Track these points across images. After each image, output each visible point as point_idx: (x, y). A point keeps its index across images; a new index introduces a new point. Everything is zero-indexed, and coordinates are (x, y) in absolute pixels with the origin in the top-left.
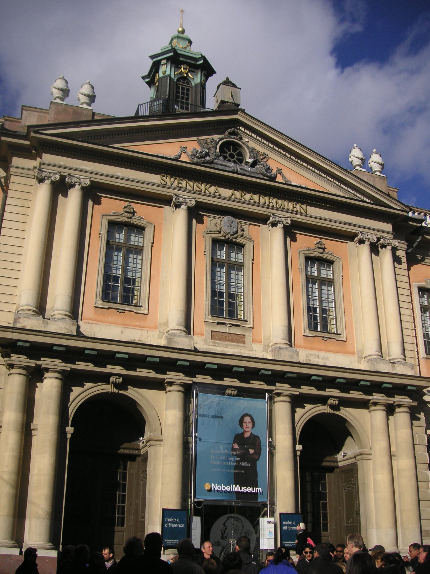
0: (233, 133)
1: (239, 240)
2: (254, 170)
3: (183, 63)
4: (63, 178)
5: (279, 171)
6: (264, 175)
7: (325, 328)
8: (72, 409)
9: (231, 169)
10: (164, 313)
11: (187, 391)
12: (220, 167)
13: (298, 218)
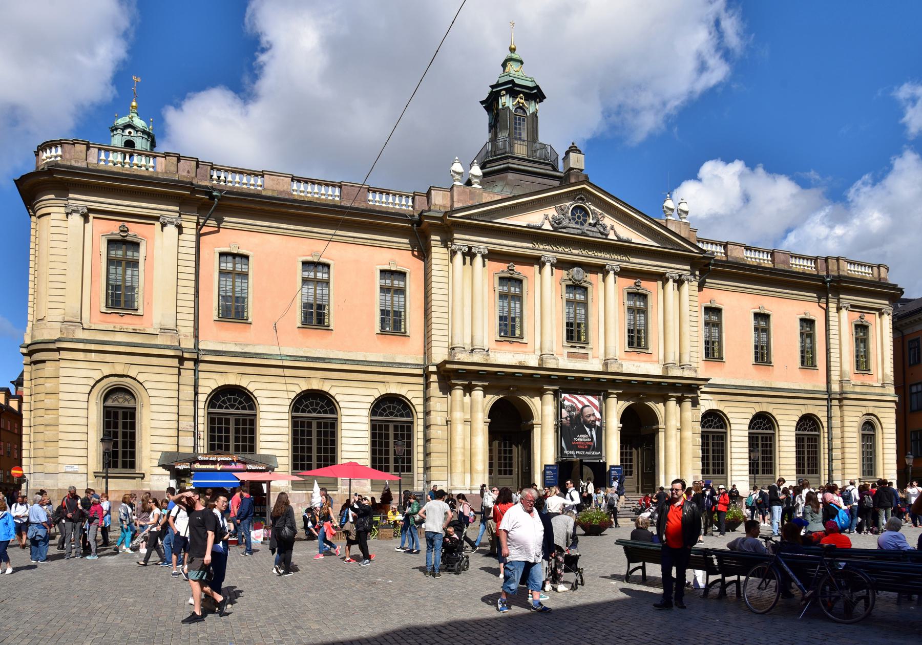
1: (584, 284)
2: (595, 229)
4: (470, 248)
6: (602, 233)
7: (639, 344)
9: (579, 231)
10: (542, 343)
12: (572, 231)
13: (625, 265)
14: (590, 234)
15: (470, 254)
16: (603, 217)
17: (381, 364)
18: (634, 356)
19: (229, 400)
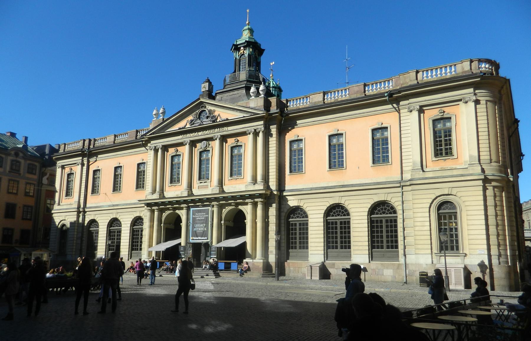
0: (202, 107)
1: (208, 149)
2: (207, 120)
3: (240, 48)
5: (219, 115)
11: (188, 208)
14: (204, 123)
15: (156, 151)
16: (214, 111)
17: (135, 204)
18: (233, 182)
19: (382, 209)
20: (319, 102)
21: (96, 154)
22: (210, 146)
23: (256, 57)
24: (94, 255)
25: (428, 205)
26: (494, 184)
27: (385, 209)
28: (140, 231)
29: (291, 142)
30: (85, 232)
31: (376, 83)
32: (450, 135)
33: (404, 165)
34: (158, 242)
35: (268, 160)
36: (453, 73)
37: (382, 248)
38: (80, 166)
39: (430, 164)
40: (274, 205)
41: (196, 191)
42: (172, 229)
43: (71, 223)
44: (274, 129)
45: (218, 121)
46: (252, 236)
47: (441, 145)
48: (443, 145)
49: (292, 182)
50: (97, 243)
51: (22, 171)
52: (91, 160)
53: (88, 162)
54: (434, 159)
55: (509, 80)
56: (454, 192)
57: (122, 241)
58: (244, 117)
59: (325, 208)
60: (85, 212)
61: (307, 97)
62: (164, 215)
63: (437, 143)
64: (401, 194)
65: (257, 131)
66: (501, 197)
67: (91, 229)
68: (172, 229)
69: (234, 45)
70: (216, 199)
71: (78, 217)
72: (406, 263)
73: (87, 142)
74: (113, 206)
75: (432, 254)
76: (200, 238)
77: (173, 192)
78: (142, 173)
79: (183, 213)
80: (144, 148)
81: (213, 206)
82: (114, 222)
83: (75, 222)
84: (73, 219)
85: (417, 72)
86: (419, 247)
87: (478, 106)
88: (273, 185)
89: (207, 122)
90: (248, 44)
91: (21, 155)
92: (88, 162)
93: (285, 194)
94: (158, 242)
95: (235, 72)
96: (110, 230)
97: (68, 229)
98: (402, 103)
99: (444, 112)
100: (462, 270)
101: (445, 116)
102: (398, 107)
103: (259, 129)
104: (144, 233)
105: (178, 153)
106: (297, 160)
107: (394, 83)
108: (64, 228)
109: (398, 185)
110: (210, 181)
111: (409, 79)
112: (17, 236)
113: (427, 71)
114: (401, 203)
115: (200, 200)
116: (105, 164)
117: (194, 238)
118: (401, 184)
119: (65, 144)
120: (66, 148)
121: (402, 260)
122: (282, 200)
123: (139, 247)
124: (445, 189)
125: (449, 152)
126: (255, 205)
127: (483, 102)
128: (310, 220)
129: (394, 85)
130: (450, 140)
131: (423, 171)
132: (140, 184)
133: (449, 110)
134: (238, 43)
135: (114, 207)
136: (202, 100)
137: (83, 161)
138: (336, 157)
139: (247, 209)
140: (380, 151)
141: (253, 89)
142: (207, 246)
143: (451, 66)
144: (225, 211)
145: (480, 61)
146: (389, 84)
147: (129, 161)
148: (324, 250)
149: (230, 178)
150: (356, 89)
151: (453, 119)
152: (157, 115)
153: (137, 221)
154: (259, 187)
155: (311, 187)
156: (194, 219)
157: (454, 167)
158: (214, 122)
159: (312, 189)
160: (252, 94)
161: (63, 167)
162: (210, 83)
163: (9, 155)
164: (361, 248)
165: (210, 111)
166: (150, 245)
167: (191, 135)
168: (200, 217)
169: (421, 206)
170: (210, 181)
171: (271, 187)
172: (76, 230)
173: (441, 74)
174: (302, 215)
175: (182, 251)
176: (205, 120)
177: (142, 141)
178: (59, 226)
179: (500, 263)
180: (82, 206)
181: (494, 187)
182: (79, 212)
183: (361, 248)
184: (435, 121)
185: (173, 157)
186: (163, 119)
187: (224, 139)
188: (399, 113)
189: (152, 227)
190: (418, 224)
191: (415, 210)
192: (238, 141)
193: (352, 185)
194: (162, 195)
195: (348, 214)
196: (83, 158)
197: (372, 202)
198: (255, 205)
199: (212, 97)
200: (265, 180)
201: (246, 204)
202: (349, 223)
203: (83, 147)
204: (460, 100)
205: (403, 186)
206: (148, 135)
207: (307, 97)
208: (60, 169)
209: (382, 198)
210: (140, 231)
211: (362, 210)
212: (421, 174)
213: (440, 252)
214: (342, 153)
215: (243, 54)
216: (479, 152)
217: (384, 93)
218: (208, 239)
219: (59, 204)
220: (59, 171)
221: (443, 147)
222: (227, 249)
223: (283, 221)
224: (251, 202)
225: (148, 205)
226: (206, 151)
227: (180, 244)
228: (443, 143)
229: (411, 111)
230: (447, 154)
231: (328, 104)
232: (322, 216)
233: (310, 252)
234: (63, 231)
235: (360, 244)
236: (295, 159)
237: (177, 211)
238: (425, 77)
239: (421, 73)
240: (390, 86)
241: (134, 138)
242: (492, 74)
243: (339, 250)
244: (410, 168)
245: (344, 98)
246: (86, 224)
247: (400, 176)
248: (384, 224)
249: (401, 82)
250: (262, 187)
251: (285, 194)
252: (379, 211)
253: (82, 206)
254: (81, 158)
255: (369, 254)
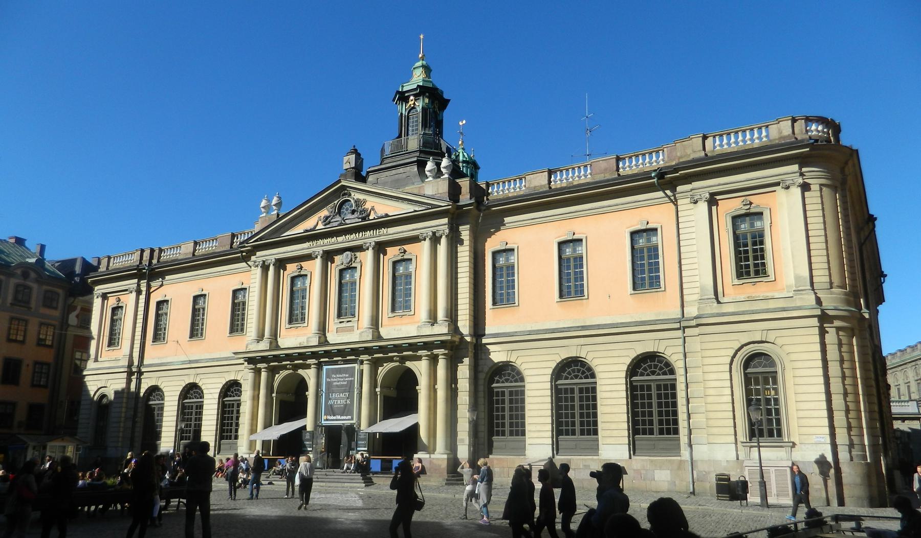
2: (353, 216)
3: (409, 97)
4: (264, 262)
5: (373, 209)
8: (276, 385)
11: (319, 366)
14: (347, 221)
15: (265, 268)
16: (365, 201)
18: (397, 320)
19: (650, 367)
20: (541, 186)
21: (162, 275)
22: (358, 260)
23: (435, 112)
24: (155, 447)
25: (728, 360)
26: (837, 323)
27: (656, 366)
28: (235, 406)
29: (495, 254)
30: (141, 408)
31: (637, 156)
32: (762, 243)
33: (685, 292)
34: (267, 425)
35: (457, 283)
36: (765, 139)
37: (651, 433)
38: (134, 294)
39: (729, 290)
40: (466, 361)
41: (332, 337)
42: (290, 403)
43: (116, 393)
44: (465, 232)
45: (371, 218)
46: (429, 414)
47: (747, 259)
48: (750, 258)
49: (496, 321)
50: (161, 426)
51: (33, 304)
52: (152, 284)
53: (149, 287)
54: (736, 282)
55: (857, 151)
56: (771, 337)
57: (203, 423)
58: (415, 211)
59: (554, 365)
60: (140, 373)
61: (521, 179)
62: (278, 378)
63: (740, 256)
64: (681, 341)
65: (437, 235)
66: (851, 345)
67: (151, 403)
68: (290, 403)
69: (398, 92)
70: (367, 351)
71: (129, 381)
72: (692, 459)
73: (147, 254)
74: (190, 362)
75: (736, 443)
76: (339, 417)
77: (293, 339)
78: (241, 307)
79: (309, 375)
80: (244, 264)
81: (362, 362)
82: (192, 391)
83: (123, 390)
84: (120, 384)
85: (705, 138)
86: (715, 431)
87: (807, 194)
88: (464, 326)
89: (352, 220)
90: (422, 91)
91: (33, 275)
92: (149, 287)
93: (484, 341)
94: (267, 425)
95: (400, 136)
96: (183, 404)
97: (111, 402)
98: (680, 188)
99: (751, 203)
100: (788, 470)
101: (752, 210)
102: (674, 195)
103: (441, 232)
104: (242, 409)
105: (302, 273)
106: (572, 277)
107: (666, 156)
108: (105, 401)
109: (677, 326)
110: (356, 319)
111: (691, 149)
112: (21, 415)
113: (721, 135)
114: (682, 356)
115: (340, 353)
116: (177, 291)
117: (329, 417)
118: (682, 325)
119: (109, 258)
120: (111, 264)
121: (685, 453)
122: (479, 351)
123: (233, 434)
124: (755, 332)
125: (760, 271)
126: (434, 360)
127: (815, 187)
128: (528, 386)
129: (666, 159)
130: (762, 250)
131: (719, 302)
132: (237, 325)
133: (759, 201)
134: (405, 89)
135: (192, 365)
136: (344, 183)
137: (139, 285)
138: (571, 279)
139: (420, 368)
140: (645, 269)
141: (430, 166)
142: (351, 431)
143: (760, 128)
144: (382, 371)
145: (808, 120)
146: (658, 157)
147: (218, 285)
148: (552, 438)
149: (391, 315)
150: (603, 165)
151: (766, 214)
152: (268, 208)
153: (231, 388)
154: (441, 329)
155: (529, 328)
156: (328, 384)
157: (770, 295)
158: (364, 219)
159: (530, 333)
160: (428, 174)
161: (105, 297)
162: (358, 156)
163: (11, 275)
164: (615, 433)
165: (358, 202)
166: (253, 430)
167: (325, 241)
168: (339, 380)
169: (714, 361)
170: (356, 319)
171: (461, 329)
172: (124, 405)
173: (744, 141)
174: (513, 377)
175: (308, 440)
176: (350, 216)
177: (242, 252)
178: (95, 398)
179: (852, 459)
180: (136, 363)
181: (838, 329)
182: (130, 374)
183: (615, 433)
184: (736, 219)
185: (293, 279)
186: (278, 215)
187: (380, 248)
188: (676, 205)
189: (256, 398)
190: (711, 392)
191: (706, 369)
192: (405, 251)
193: (599, 327)
194: (274, 344)
195: (593, 376)
196: (139, 281)
197: (634, 355)
198: (434, 360)
199: (360, 178)
200: (451, 318)
201: (419, 358)
202: (594, 390)
203: (141, 263)
204: (778, 184)
205: (684, 328)
206: (252, 243)
207: (521, 179)
208: (100, 299)
209: (649, 348)
210: (235, 406)
211: (616, 368)
212: (714, 308)
213: (750, 440)
214: (582, 272)
215: (414, 108)
216: (811, 270)
217: (650, 172)
218: (352, 419)
219: (96, 360)
220: (97, 303)
221: (751, 262)
222: (385, 436)
223: (481, 388)
224: (426, 356)
225: (250, 361)
226: (350, 268)
227: (304, 427)
228: (751, 254)
229: (696, 202)
230: (757, 273)
231: (556, 189)
232: (548, 378)
233: (528, 441)
234: (102, 407)
235: (613, 426)
236: (501, 282)
237: (300, 371)
238: (717, 146)
239: (710, 140)
240: (659, 161)
241: (228, 247)
242: (829, 141)
243: (578, 436)
244: (696, 297)
245: (583, 180)
246: (142, 394)
247: (679, 309)
248: (654, 392)
249: (679, 154)
250: (445, 330)
251: (484, 341)
252: (645, 369)
253: (136, 363)
254: (136, 281)
255: (629, 444)
